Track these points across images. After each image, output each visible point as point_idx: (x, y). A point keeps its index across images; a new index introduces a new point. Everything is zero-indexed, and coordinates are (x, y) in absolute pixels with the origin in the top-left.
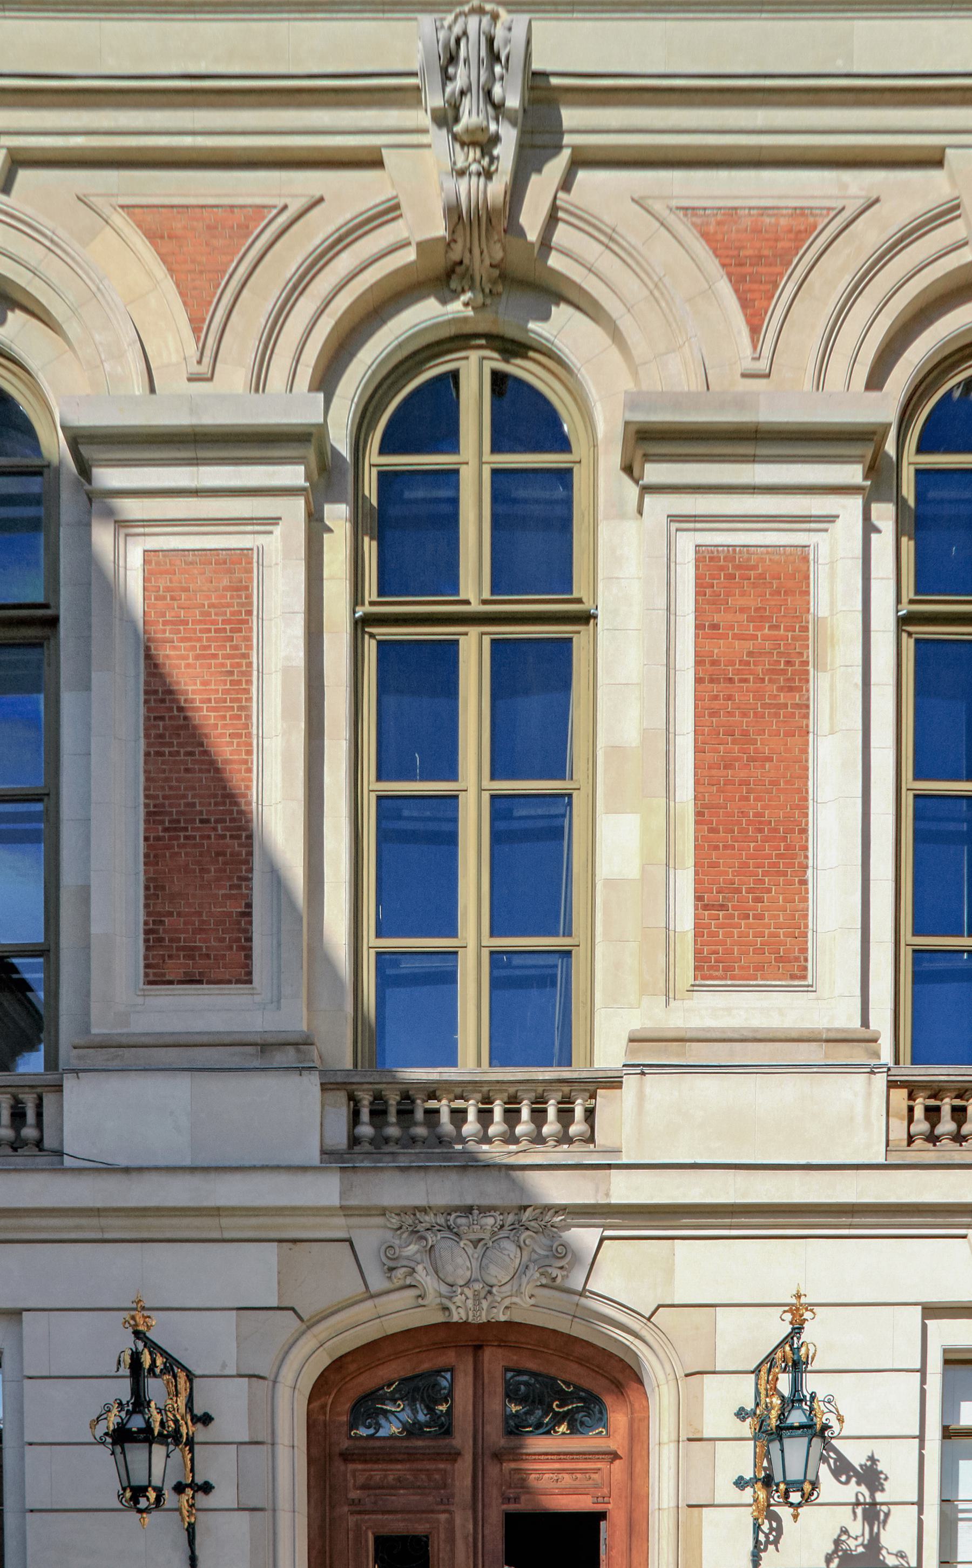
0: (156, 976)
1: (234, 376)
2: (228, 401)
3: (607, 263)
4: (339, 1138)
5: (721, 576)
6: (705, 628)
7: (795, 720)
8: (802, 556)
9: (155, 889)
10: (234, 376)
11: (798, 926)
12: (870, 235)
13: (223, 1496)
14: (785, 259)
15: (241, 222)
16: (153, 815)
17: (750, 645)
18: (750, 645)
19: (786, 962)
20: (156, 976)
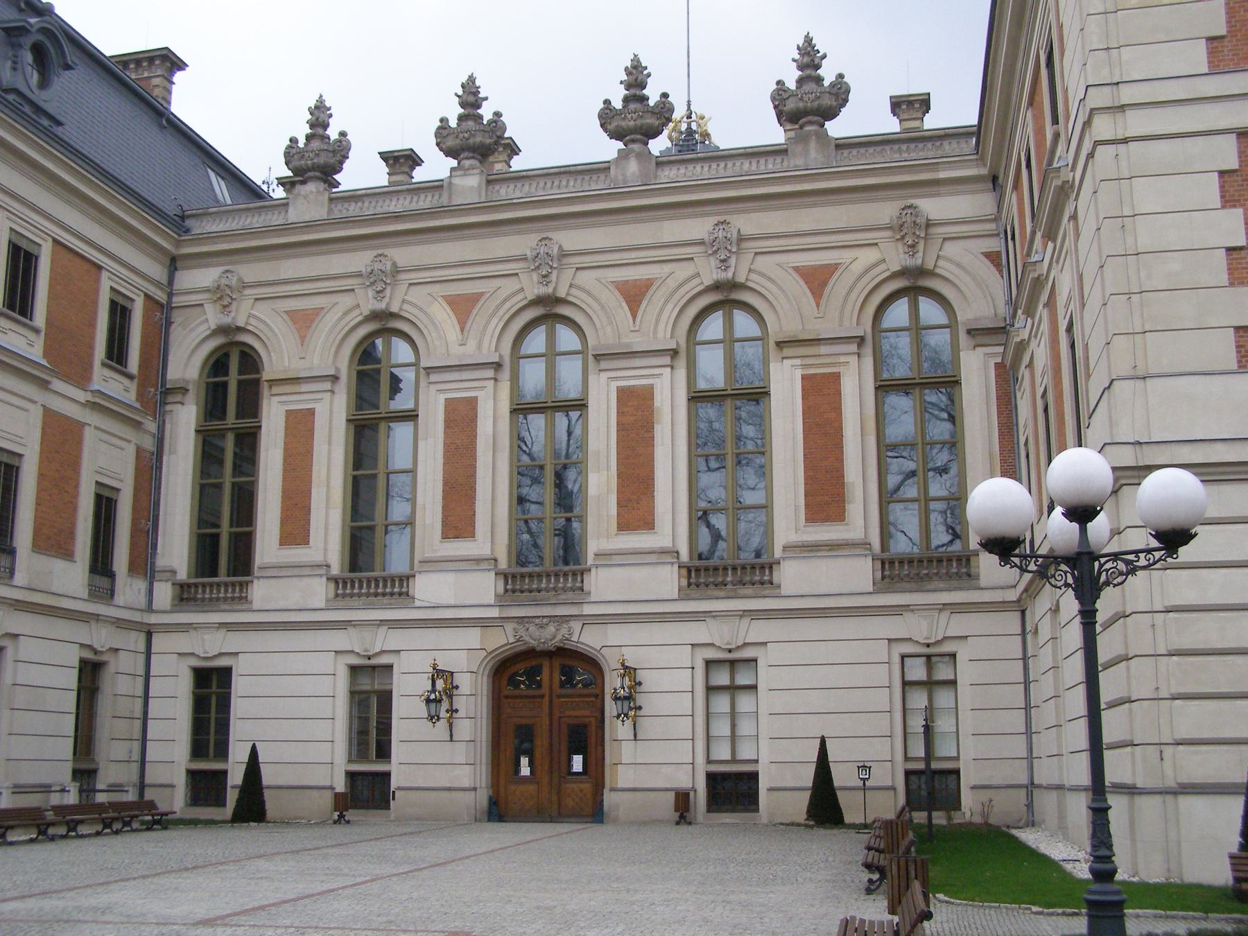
0: (446, 536)
1: (472, 344)
2: (469, 353)
3: (589, 300)
4: (501, 589)
5: (625, 395)
6: (620, 413)
7: (649, 442)
8: (651, 387)
9: (445, 508)
10: (472, 344)
11: (651, 511)
12: (671, 284)
13: (462, 713)
14: (643, 294)
15: (475, 298)
16: (445, 483)
17: (633, 418)
18: (633, 418)
19: (648, 524)
20: (446, 536)
